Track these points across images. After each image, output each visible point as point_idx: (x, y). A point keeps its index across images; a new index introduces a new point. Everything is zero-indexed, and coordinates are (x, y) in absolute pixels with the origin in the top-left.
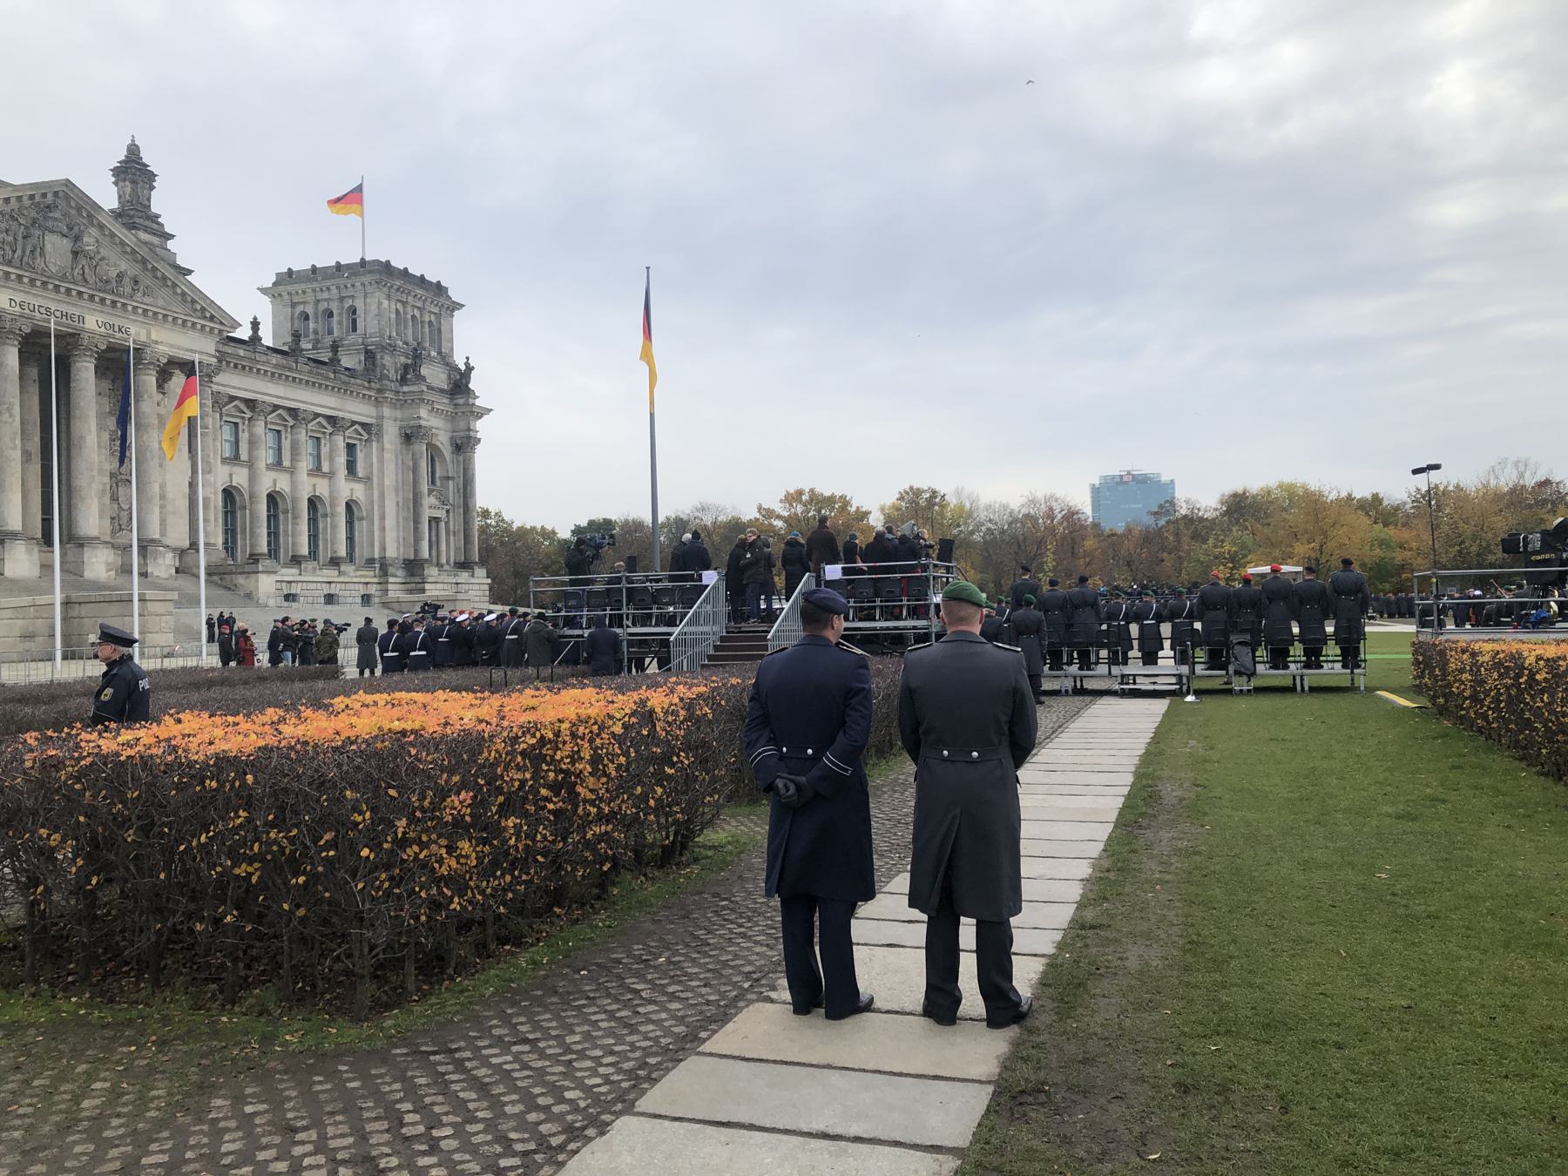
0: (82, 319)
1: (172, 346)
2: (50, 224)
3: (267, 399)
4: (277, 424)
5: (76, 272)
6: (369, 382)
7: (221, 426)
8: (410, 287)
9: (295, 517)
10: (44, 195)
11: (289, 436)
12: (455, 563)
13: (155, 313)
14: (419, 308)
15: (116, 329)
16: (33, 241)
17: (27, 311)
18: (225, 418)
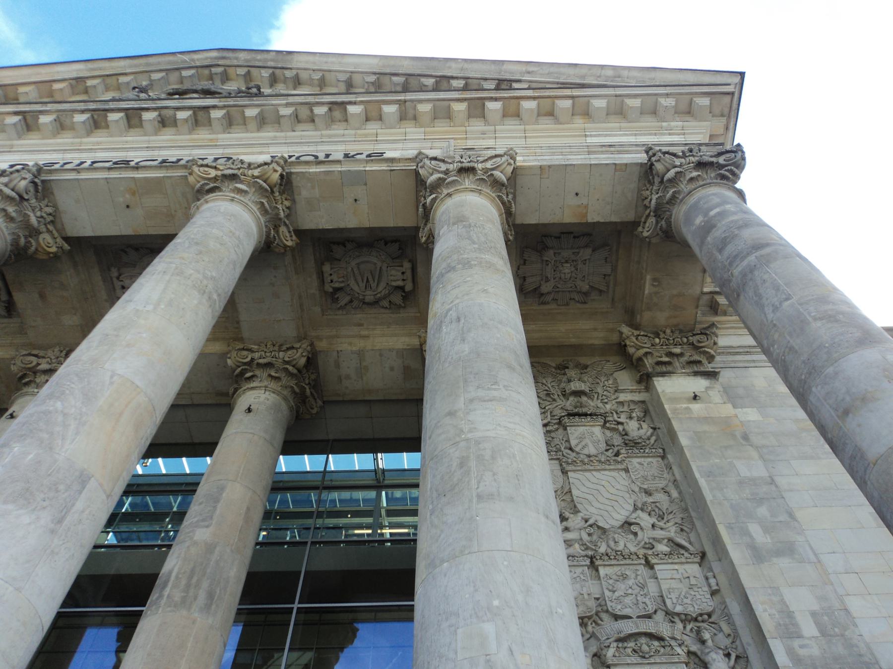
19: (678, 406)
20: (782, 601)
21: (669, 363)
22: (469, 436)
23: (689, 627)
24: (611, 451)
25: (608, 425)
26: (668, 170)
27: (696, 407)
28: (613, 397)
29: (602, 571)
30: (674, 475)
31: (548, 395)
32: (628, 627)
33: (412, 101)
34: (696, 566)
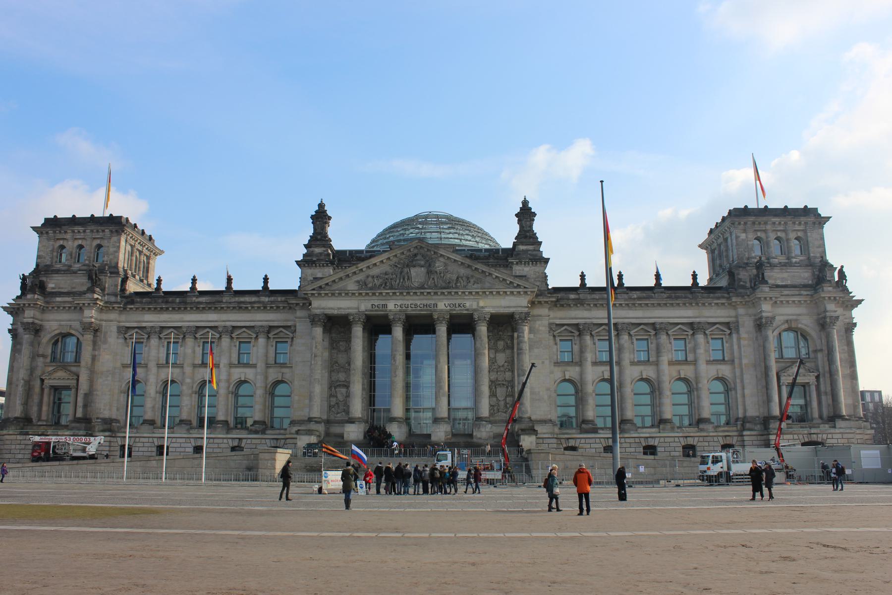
0: (436, 305)
1: (493, 307)
3: (626, 321)
4: (643, 335)
5: (429, 283)
6: (728, 293)
7: (594, 344)
8: (765, 219)
9: (660, 394)
10: (410, 250)
11: (654, 341)
12: (829, 417)
13: (477, 293)
14: (784, 231)
15: (457, 306)
16: (403, 274)
17: (404, 308)
18: (596, 338)
32: (500, 383)
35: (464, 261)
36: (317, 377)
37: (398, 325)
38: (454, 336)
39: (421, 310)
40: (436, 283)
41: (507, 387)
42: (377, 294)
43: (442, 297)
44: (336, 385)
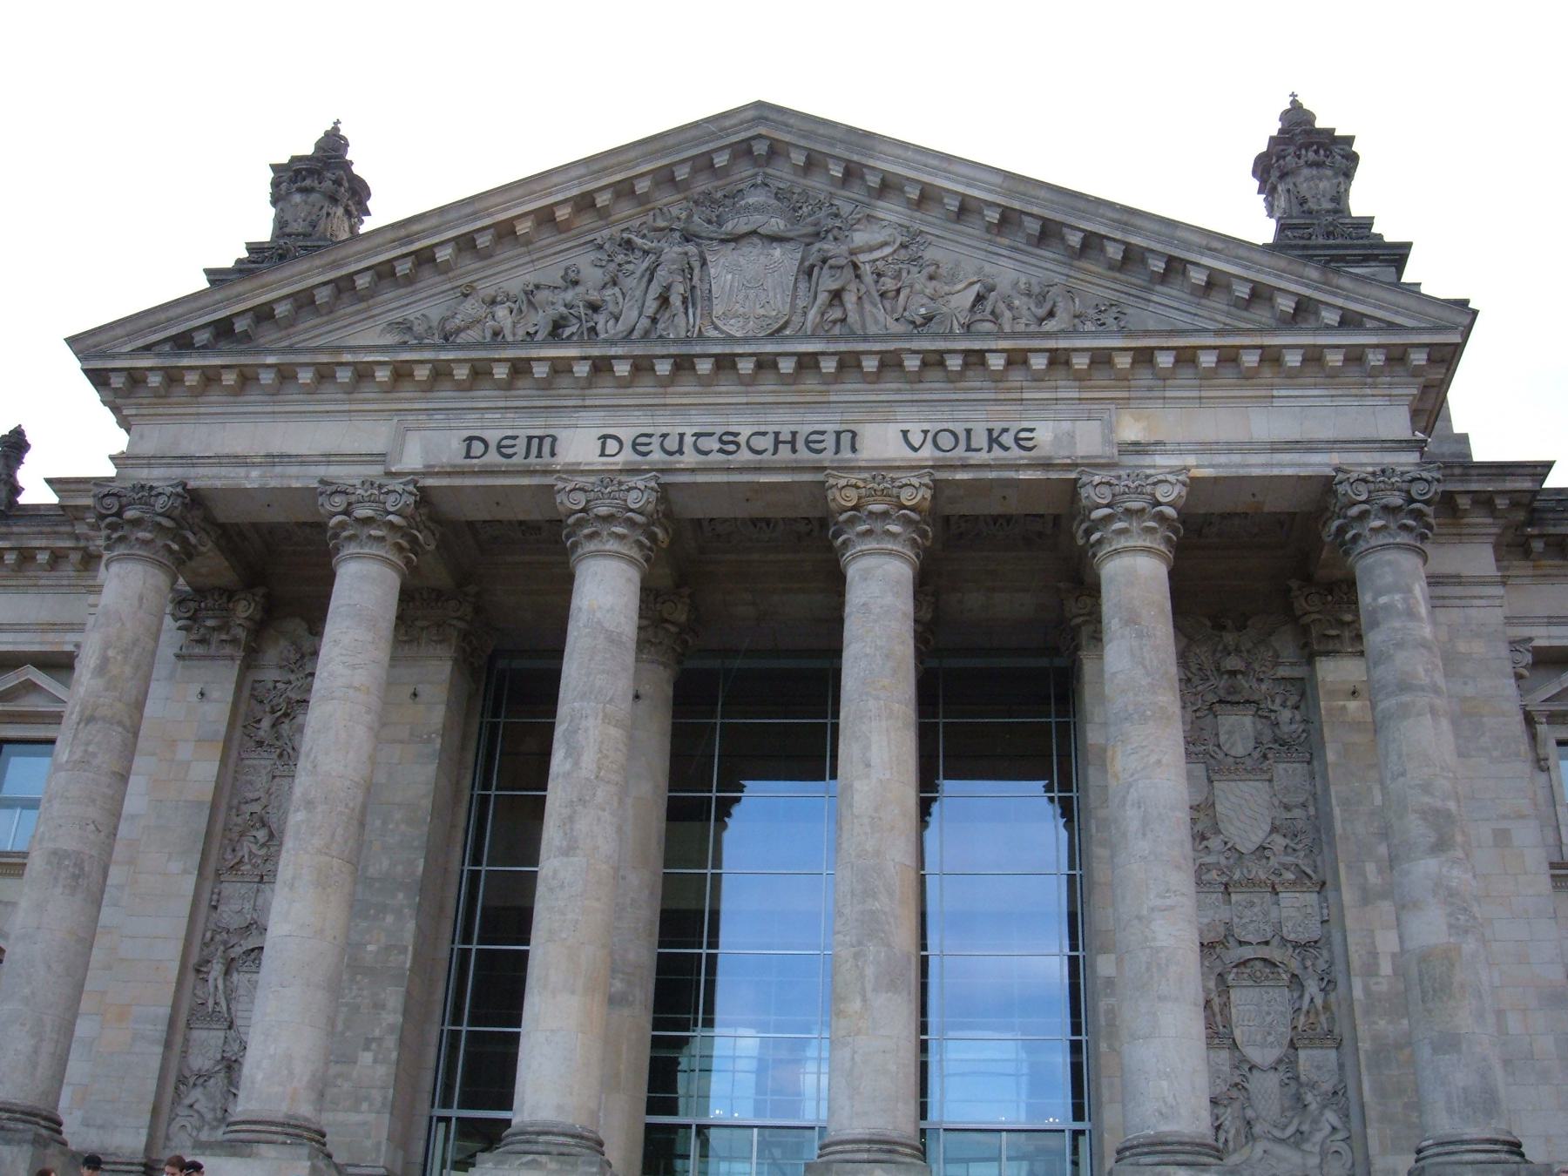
1: (1205, 448)
2: (732, 226)
5: (812, 314)
13: (1101, 359)
15: (980, 440)
16: (661, 273)
19: (1335, 703)
20: (1373, 943)
21: (1338, 636)
22: (1152, 944)
23: (1297, 951)
24: (1259, 750)
25: (1260, 713)
26: (1354, 504)
27: (1353, 705)
28: (1272, 673)
29: (1234, 897)
30: (1315, 785)
31: (1200, 669)
32: (1247, 952)
33: (1065, 349)
34: (1315, 896)
35: (1017, 205)
36: (68, 843)
37: (612, 545)
38: (949, 787)
39: (758, 469)
40: (853, 317)
41: (1296, 981)
42: (501, 372)
43: (890, 389)
44: (236, 952)
